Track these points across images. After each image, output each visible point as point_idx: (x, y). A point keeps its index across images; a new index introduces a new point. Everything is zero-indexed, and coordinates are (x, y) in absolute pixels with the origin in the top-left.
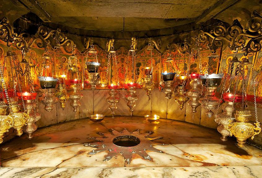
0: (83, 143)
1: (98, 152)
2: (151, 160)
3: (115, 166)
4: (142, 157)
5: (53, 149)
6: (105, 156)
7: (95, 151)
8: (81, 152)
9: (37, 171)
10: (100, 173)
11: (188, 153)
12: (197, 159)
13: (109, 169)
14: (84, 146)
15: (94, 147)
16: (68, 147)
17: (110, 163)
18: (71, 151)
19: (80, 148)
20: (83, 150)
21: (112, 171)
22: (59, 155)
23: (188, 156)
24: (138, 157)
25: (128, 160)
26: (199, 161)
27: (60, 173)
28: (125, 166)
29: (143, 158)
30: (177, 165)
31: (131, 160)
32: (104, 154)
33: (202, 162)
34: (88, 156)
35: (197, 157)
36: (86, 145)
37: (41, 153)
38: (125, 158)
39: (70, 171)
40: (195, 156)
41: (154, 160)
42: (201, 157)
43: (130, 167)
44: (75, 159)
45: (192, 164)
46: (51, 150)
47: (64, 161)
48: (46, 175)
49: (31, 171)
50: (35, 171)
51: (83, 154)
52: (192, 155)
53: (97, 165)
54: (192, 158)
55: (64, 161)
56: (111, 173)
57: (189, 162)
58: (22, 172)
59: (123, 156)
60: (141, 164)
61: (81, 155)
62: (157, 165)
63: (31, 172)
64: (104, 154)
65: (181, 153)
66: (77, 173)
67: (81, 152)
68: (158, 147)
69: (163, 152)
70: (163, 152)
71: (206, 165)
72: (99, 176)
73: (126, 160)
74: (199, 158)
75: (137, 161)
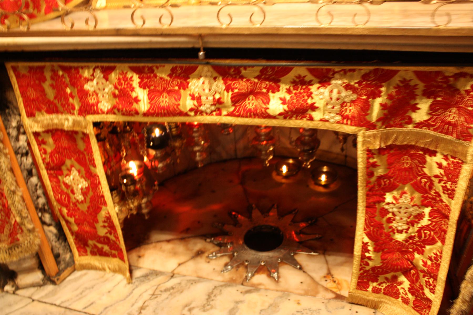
0: (204, 236)
1: (219, 255)
3: (231, 282)
4: (268, 273)
6: (226, 265)
8: (199, 253)
9: (153, 279)
10: (211, 291)
11: (332, 276)
12: (335, 288)
13: (220, 288)
14: (205, 240)
17: (227, 275)
18: (188, 249)
20: (203, 249)
21: (223, 291)
22: (175, 254)
23: (329, 281)
25: (250, 275)
26: (335, 290)
28: (242, 284)
29: (269, 276)
30: (302, 292)
31: (253, 275)
33: (338, 292)
34: (206, 261)
35: (339, 284)
36: (208, 240)
37: (155, 247)
39: (183, 284)
40: (337, 282)
41: (280, 280)
45: (322, 294)
47: (179, 265)
48: (162, 285)
49: (149, 277)
50: (151, 278)
51: (201, 257)
52: (335, 279)
55: (179, 265)
57: (321, 290)
58: (141, 278)
60: (260, 284)
62: (279, 289)
63: (149, 279)
65: (324, 272)
66: (189, 288)
68: (302, 257)
69: (301, 268)
70: (301, 268)
73: (247, 275)
74: (339, 287)
75: (261, 278)
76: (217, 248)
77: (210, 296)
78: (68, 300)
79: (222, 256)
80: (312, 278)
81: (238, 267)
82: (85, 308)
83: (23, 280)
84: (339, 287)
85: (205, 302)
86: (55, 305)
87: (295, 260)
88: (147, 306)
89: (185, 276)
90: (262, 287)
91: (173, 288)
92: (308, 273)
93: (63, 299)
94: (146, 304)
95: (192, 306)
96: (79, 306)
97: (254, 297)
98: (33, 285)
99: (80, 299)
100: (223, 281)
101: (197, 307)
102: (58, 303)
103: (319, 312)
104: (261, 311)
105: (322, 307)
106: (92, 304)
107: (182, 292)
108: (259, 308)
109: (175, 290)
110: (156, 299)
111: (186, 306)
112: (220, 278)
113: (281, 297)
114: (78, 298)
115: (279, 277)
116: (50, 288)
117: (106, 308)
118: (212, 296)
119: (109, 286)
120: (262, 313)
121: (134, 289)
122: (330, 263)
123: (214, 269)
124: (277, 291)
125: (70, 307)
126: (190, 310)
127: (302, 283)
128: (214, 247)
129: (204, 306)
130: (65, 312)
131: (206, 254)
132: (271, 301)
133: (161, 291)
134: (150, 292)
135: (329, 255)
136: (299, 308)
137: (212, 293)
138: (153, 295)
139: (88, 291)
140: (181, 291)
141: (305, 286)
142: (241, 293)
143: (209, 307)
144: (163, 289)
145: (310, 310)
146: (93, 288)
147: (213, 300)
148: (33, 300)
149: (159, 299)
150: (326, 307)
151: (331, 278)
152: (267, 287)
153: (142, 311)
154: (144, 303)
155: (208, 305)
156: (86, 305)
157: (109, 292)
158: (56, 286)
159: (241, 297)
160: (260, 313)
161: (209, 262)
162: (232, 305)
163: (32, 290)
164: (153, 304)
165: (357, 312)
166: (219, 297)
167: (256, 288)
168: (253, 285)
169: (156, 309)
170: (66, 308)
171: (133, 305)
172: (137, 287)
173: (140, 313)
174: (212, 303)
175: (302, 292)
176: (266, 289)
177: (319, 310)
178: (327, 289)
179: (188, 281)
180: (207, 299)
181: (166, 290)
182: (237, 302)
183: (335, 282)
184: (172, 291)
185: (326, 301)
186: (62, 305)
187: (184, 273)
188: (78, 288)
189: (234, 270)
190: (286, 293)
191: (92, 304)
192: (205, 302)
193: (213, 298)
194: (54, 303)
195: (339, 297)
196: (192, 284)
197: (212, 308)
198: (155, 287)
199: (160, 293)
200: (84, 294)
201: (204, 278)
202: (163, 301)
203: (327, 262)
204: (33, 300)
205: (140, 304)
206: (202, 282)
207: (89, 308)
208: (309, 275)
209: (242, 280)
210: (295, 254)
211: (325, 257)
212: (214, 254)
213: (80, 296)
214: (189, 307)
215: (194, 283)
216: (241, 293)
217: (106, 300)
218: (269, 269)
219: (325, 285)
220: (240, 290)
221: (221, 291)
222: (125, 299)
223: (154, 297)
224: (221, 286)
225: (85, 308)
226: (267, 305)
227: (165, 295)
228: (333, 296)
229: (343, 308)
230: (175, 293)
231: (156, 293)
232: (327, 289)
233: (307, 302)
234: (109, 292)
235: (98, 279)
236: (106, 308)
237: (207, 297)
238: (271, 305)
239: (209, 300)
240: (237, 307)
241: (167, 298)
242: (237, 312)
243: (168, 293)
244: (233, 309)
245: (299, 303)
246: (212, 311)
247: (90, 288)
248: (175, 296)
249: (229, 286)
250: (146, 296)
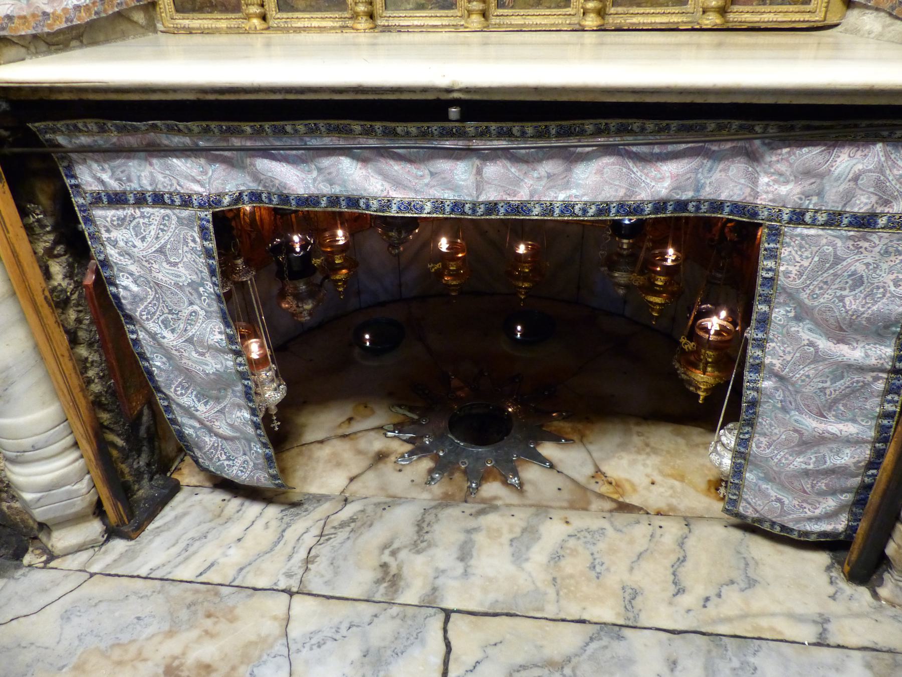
1: (415, 457)
2: (519, 488)
3: (447, 501)
4: (503, 478)
5: (321, 442)
6: (431, 472)
7: (411, 453)
8: (381, 457)
9: (315, 508)
10: (419, 518)
11: (604, 474)
13: (434, 511)
14: (385, 434)
15: (408, 441)
16: (352, 436)
17: (437, 489)
18: (359, 452)
19: (378, 443)
20: (385, 449)
21: (440, 515)
23: (601, 483)
24: (495, 479)
26: (615, 496)
27: (355, 514)
28: (466, 502)
29: (505, 483)
30: (565, 504)
31: (479, 485)
32: (426, 464)
33: (621, 500)
34: (395, 470)
35: (617, 485)
36: (390, 434)
38: (468, 480)
39: (370, 509)
41: (526, 487)
42: (627, 487)
43: (475, 502)
44: (370, 476)
45: (596, 504)
46: (319, 445)
47: (352, 480)
48: (333, 517)
50: (311, 508)
51: (385, 463)
52: (610, 479)
53: (414, 495)
54: (604, 489)
55: (352, 480)
56: (438, 520)
57: (593, 498)
59: (465, 472)
60: (495, 498)
61: (381, 466)
63: (306, 510)
64: (426, 464)
65: (589, 470)
66: (381, 516)
67: (381, 457)
68: (548, 450)
70: (552, 466)
71: (624, 507)
72: (418, 525)
74: (620, 490)
75: (492, 489)
76: (409, 447)
77: (421, 527)
78: (164, 565)
79: (419, 458)
80: (573, 481)
81: (451, 474)
82: (201, 574)
83: (61, 540)
84: (620, 490)
85: (415, 538)
86: (138, 577)
87: (540, 454)
88: (317, 556)
89: (366, 498)
90: (499, 503)
91: (353, 520)
92: (565, 472)
93: (152, 565)
94: (313, 553)
95: (395, 546)
96: (187, 572)
97: (491, 520)
98: (80, 548)
99: (186, 559)
100: (433, 500)
101: (405, 547)
102: (143, 572)
103: (603, 534)
104: (511, 540)
105: (605, 524)
106: (212, 565)
107: (371, 525)
108: (506, 537)
109: (359, 523)
110: (329, 542)
111: (385, 547)
112: (426, 496)
113: (537, 515)
114: (181, 558)
115: (521, 484)
116: (119, 545)
117: (241, 569)
118: (425, 525)
119: (235, 530)
120: (514, 544)
121: (284, 531)
122: (595, 455)
123: (413, 481)
124: (525, 506)
125: (170, 577)
126: (394, 554)
127: (559, 489)
128: (402, 445)
129: (415, 544)
130: (162, 587)
131: (393, 458)
132: (523, 524)
133: (334, 528)
134: (316, 531)
135: (591, 443)
136: (569, 529)
137: (423, 520)
138: (321, 536)
139: (197, 544)
140: (369, 523)
141: (566, 495)
142: (471, 515)
143: (425, 544)
144: (336, 524)
145: (588, 530)
146: (206, 537)
147: (427, 532)
148: (92, 575)
149: (335, 542)
150: (612, 523)
151: (603, 478)
152: (508, 501)
153: (310, 566)
154: (309, 553)
155: (422, 542)
156: (201, 570)
157: (239, 540)
158: (132, 543)
159: (472, 523)
160: (511, 545)
161: (400, 471)
162: (462, 537)
163: (84, 556)
164: (324, 551)
165: (661, 527)
166: (436, 527)
167: (489, 507)
168: (483, 501)
169: (334, 559)
170: (161, 579)
171: (290, 557)
172: (289, 525)
173: (307, 569)
174: (427, 537)
175: (565, 504)
176: (508, 506)
177: (602, 529)
178: (601, 496)
179: (377, 505)
180: (418, 532)
181: (343, 525)
182: (469, 531)
183: (611, 483)
184: (353, 525)
185: (607, 515)
186: (151, 576)
187: (363, 492)
188: (177, 542)
189: (445, 480)
190: (542, 509)
191: (212, 565)
192: (415, 538)
193: (426, 529)
194: (135, 574)
195: (624, 507)
196: (384, 509)
197: (429, 546)
198: (323, 522)
199: (333, 531)
200: (191, 549)
201: (400, 498)
202: (342, 543)
203: (590, 453)
204: (92, 575)
205: (302, 554)
206: (400, 504)
207: (208, 572)
208: (568, 477)
209: (463, 494)
210: (537, 444)
211: (584, 445)
212: (406, 455)
213: (186, 554)
214: (391, 549)
215: (387, 508)
216: (471, 515)
217: (236, 556)
218: (506, 472)
219: (597, 490)
220: (468, 512)
221: (436, 515)
222: (272, 550)
223: (323, 538)
224: (435, 507)
225: (201, 574)
226: (518, 530)
227: (343, 534)
228: (614, 505)
229: (638, 522)
230: (359, 528)
231: (325, 532)
232: (601, 496)
233: (580, 521)
234: (239, 540)
235: (210, 521)
236: (241, 569)
237: (416, 529)
238: (524, 530)
239: (421, 533)
240: (471, 540)
241: (348, 538)
242: (473, 547)
243: (348, 529)
244: (465, 542)
245: (567, 522)
246: (432, 551)
247: (200, 539)
248: (361, 534)
249: (447, 506)
250: (309, 540)
